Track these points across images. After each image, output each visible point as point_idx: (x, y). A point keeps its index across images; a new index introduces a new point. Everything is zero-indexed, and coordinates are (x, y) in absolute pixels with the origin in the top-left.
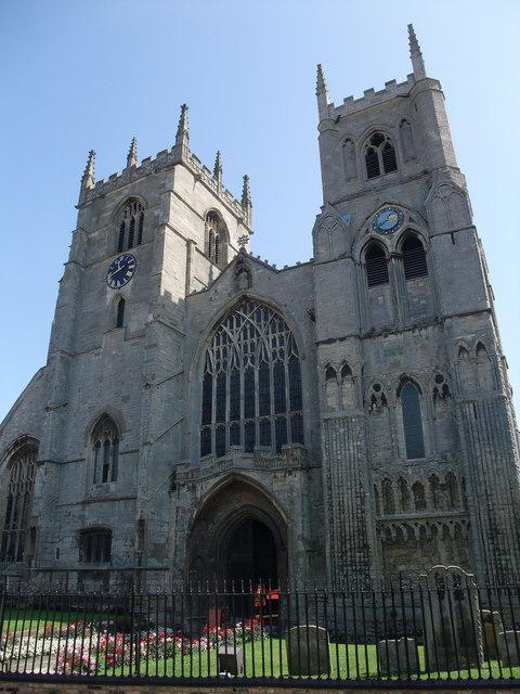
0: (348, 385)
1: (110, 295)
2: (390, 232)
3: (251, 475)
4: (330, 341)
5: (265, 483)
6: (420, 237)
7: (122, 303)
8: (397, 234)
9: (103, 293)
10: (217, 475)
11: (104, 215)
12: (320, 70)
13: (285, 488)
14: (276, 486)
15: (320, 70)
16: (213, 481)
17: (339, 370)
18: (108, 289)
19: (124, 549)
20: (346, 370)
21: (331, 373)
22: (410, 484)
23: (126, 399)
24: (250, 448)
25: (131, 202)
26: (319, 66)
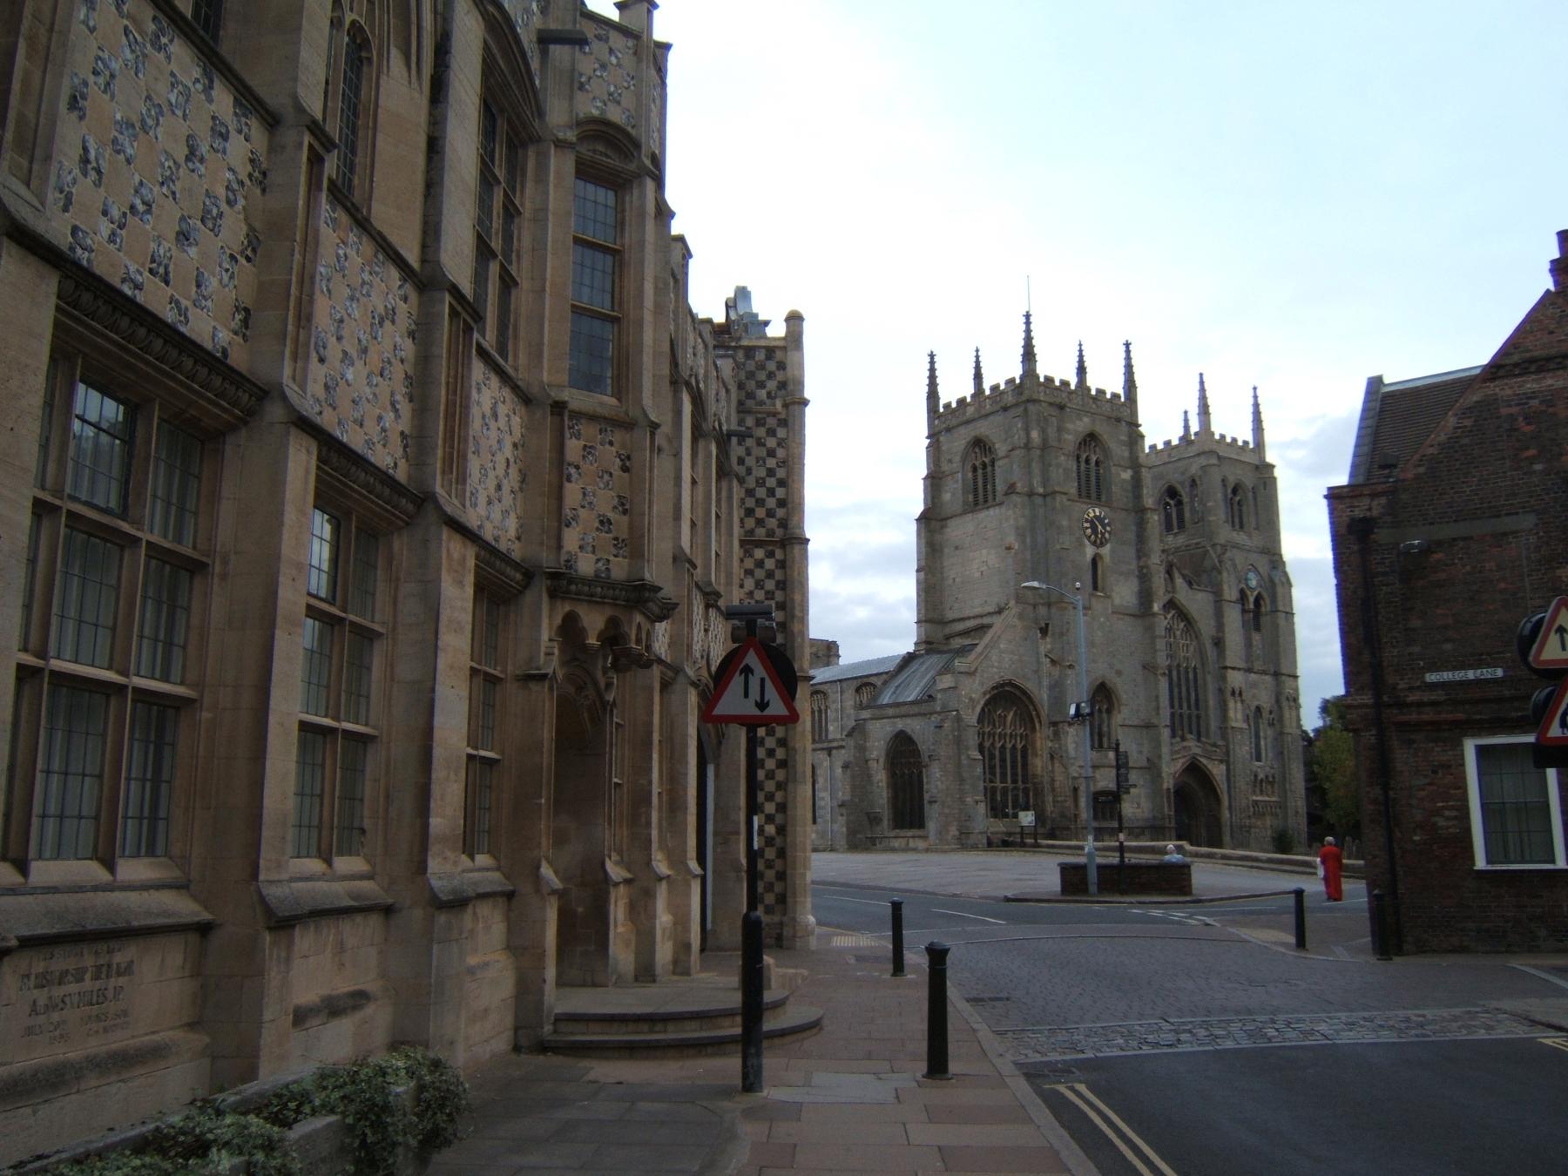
0: (1239, 704)
1: (1090, 551)
2: (1252, 589)
3: (1202, 760)
4: (1233, 668)
5: (1209, 767)
6: (1262, 602)
7: (1094, 562)
8: (1256, 593)
9: (1082, 545)
10: (1184, 757)
11: (1066, 436)
12: (1202, 383)
13: (1217, 771)
14: (1215, 771)
15: (1202, 383)
16: (1181, 761)
17: (1237, 692)
18: (1087, 542)
19: (1131, 810)
20: (1240, 694)
21: (1233, 693)
22: (1259, 778)
23: (1119, 673)
24: (1199, 740)
25: (1091, 438)
26: (1201, 375)
